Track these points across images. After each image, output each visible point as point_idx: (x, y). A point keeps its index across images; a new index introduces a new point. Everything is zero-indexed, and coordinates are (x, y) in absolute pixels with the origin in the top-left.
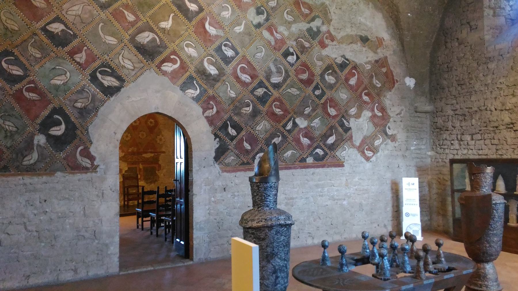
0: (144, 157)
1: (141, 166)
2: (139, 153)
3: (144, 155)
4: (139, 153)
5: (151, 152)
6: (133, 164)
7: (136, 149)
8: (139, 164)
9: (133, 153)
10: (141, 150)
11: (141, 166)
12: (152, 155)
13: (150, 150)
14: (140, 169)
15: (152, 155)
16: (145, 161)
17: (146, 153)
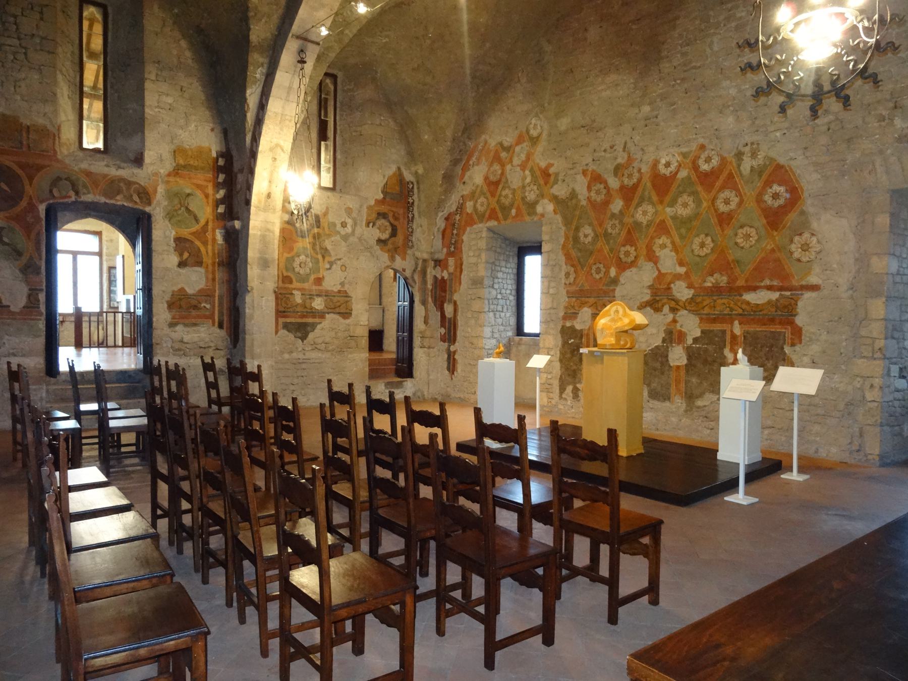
0: (748, 303)
1: (737, 329)
2: (733, 290)
3: (750, 297)
4: (733, 290)
5: (770, 288)
6: (714, 321)
7: (725, 279)
8: (732, 323)
9: (717, 290)
10: (740, 283)
11: (737, 329)
12: (775, 296)
13: (767, 282)
14: (734, 337)
15: (775, 296)
16: (751, 315)
17: (754, 289)
